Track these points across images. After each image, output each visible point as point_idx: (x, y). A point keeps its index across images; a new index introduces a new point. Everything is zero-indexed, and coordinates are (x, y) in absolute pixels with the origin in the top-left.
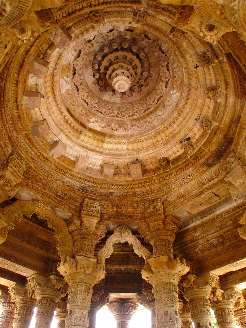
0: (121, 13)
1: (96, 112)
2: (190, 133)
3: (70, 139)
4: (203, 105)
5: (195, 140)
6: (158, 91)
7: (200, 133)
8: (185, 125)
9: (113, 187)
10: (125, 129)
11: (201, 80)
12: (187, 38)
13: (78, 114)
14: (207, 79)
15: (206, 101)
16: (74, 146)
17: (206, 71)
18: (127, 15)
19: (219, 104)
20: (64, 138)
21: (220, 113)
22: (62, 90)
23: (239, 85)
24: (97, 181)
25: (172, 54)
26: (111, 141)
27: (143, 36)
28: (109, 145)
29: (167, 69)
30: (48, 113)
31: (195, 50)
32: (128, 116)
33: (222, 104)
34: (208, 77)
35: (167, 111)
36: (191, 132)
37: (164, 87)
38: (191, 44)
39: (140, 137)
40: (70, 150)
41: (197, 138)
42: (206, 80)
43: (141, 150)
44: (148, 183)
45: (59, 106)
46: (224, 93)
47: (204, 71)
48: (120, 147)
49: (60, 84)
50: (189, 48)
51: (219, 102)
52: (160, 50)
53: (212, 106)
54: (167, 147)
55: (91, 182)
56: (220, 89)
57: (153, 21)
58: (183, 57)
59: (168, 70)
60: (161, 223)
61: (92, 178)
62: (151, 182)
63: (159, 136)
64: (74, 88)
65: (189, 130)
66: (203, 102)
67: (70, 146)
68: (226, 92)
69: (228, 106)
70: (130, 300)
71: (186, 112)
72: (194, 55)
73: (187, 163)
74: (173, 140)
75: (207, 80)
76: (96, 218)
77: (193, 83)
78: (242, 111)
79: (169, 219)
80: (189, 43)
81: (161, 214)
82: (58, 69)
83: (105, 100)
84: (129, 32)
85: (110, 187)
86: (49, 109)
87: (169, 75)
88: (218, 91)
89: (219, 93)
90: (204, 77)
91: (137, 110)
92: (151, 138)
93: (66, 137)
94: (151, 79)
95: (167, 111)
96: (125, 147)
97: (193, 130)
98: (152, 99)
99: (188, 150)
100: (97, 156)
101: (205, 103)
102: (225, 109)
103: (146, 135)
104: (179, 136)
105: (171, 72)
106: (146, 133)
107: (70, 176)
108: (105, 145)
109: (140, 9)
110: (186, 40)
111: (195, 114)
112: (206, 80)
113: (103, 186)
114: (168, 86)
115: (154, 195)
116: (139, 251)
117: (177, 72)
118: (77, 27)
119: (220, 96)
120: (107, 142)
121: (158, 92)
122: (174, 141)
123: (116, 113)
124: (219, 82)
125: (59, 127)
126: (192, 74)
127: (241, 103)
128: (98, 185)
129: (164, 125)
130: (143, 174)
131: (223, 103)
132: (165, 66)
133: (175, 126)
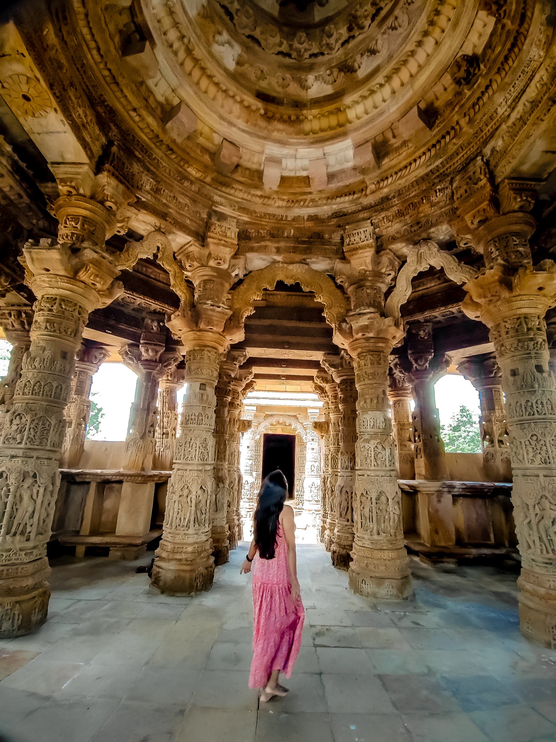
1: (313, 60)
3: (282, 143)
10: (373, 52)
13: (280, 89)
20: (274, 148)
28: (356, 109)
30: (226, 124)
32: (370, 21)
39: (404, 49)
43: (418, 72)
44: (448, 138)
55: (346, 195)
60: (485, 207)
62: (452, 133)
70: (492, 355)
76: (368, 249)
79: (506, 191)
81: (483, 187)
82: (186, 34)
83: (320, 21)
85: (381, 185)
86: (226, 115)
92: (426, 34)
93: (278, 145)
96: (387, 90)
103: (414, 33)
113: (368, 192)
115: (463, 156)
116: (457, 275)
120: (349, 107)
123: (343, 31)
125: (259, 137)
130: (430, 125)
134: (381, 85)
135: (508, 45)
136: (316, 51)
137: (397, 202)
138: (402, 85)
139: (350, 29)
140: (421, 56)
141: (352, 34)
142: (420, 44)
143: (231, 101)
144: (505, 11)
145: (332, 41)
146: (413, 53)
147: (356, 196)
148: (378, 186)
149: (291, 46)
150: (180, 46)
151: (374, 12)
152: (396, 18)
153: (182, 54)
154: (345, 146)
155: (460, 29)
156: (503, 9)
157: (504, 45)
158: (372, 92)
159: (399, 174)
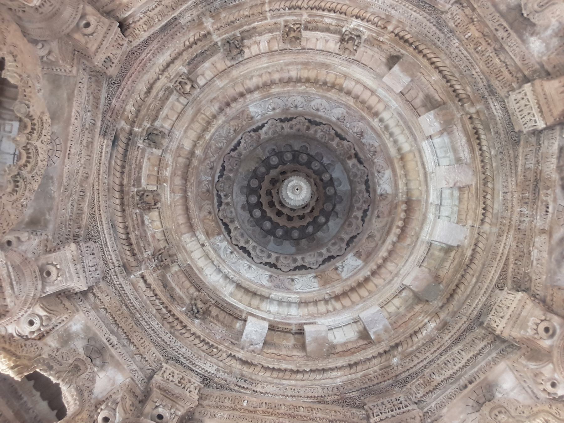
0: (187, 274)
2: (276, 48)
4: (221, 74)
5: (274, 33)
6: (278, 130)
7: (258, 38)
8: (273, 66)
9: (460, 91)
10: (362, 134)
11: (191, 112)
12: (158, 177)
14: (182, 104)
15: (213, 76)
16: (431, 203)
17: (176, 116)
18: (185, 265)
19: (189, 64)
21: (197, 49)
22: (359, 267)
23: (126, 79)
24: (469, 127)
25: (209, 162)
26: (390, 145)
27: (223, 207)
29: (239, 146)
31: (162, 154)
32: (345, 142)
33: (181, 63)
34: (179, 107)
35: (287, 100)
36: (274, 49)
37: (264, 129)
38: (159, 165)
40: (443, 206)
41: (270, 34)
42: (186, 105)
45: (380, 261)
46: (165, 76)
47: (177, 119)
48: (392, 123)
49: (350, 274)
50: (167, 164)
51: (187, 66)
52: (224, 174)
53: (207, 64)
54: (326, 60)
56: (169, 85)
57: (171, 231)
58: (192, 153)
59: (239, 143)
61: (469, 141)
63: (328, 80)
64: (354, 244)
65: (273, 55)
66: (215, 78)
67: (436, 210)
68: (160, 76)
69: (176, 51)
71: (260, 79)
72: (169, 151)
73: (314, 11)
74: (309, 62)
75: (185, 104)
77: (214, 109)
78: (150, 38)
80: (160, 168)
84: (230, 227)
85: (464, 96)
87: (244, 136)
88: (173, 83)
89: (175, 80)
90: (185, 112)
91: (327, 136)
92: (341, 90)
94: (275, 147)
95: (287, 100)
96: (385, 115)
97: (267, 51)
98: (295, 128)
99: (295, 31)
100: (427, 154)
101: (216, 74)
102: (184, 50)
104: (295, 59)
105: (239, 137)
106: (340, 101)
107: (490, 185)
108: (406, 147)
109: (154, 266)
110: (160, 175)
111: (242, 72)
112: (186, 105)
114: (260, 124)
117: (225, 137)
118: (239, 313)
119: (177, 75)
121: (278, 129)
122: (307, 59)
124: (161, 94)
126: (205, 121)
127: (145, 49)
128: (477, 122)
129: (305, 89)
131: (178, 62)
132: (237, 151)
133: (293, 74)
134: (381, 120)
135: (320, 12)
136: (364, 187)
137: (478, 70)
138: (379, 101)
139: (350, 158)
140: (358, 90)
141: (353, 156)
142: (348, 93)
143: (383, 270)
144: (294, 24)
145: (359, 173)
146: (356, 98)
147: (479, 126)
148: (465, 100)
149: (358, 209)
150: (331, 304)
151: (338, 139)
152: (338, 119)
153: (338, 305)
154: (429, 149)
155: (326, 60)
156: (292, 26)
157: (322, 17)
158: (386, 128)
159: (450, 77)
